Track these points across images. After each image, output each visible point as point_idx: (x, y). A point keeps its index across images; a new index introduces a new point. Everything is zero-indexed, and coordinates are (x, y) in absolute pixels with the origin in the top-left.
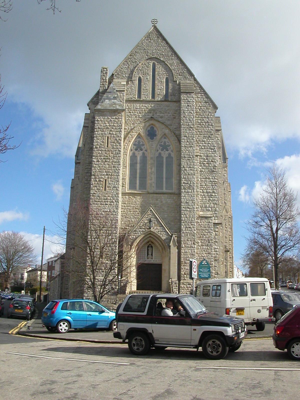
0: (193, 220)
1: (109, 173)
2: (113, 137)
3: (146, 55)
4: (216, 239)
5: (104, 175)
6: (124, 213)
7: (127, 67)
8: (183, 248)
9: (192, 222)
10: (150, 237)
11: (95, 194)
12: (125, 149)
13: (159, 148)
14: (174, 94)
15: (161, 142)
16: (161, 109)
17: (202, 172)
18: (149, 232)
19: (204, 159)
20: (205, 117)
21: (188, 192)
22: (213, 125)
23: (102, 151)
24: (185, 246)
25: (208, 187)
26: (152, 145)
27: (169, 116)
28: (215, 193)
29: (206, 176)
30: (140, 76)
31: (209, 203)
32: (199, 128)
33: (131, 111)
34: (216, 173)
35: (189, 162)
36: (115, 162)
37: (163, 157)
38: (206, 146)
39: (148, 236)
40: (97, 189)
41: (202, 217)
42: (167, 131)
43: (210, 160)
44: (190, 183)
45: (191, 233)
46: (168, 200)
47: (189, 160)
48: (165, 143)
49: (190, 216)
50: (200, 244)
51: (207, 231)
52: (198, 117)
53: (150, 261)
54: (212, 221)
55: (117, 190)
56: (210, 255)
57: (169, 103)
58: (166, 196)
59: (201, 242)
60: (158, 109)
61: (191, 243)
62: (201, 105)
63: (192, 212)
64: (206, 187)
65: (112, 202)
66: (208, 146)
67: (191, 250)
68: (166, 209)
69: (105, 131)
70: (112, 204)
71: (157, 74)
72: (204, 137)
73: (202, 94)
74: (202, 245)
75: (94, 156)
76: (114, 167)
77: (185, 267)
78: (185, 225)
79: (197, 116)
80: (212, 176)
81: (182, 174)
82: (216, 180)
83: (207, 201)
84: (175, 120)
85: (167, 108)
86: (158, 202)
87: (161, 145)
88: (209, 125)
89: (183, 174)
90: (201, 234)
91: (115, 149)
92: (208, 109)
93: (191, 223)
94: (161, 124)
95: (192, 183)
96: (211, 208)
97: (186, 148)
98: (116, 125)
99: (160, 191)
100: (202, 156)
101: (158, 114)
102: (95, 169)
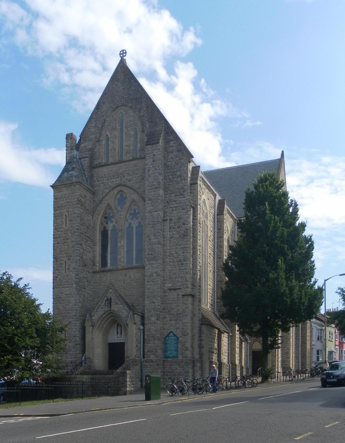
4: (185, 312)
6: (96, 293)
8: (146, 324)
9: (156, 296)
10: (112, 316)
12: (94, 225)
15: (131, 211)
16: (129, 171)
17: (173, 239)
18: (110, 312)
22: (185, 179)
23: (62, 231)
24: (149, 323)
28: (185, 261)
29: (176, 243)
30: (107, 133)
31: (180, 273)
32: (170, 186)
33: (100, 180)
34: (187, 237)
35: (154, 229)
37: (133, 227)
38: (176, 207)
39: (111, 315)
41: (170, 290)
42: (135, 196)
45: (155, 308)
47: (153, 227)
48: (135, 210)
51: (175, 305)
52: (170, 172)
53: (120, 340)
57: (137, 161)
58: (135, 270)
60: (127, 171)
61: (155, 319)
62: (172, 156)
67: (155, 326)
71: (125, 126)
73: (174, 142)
74: (171, 320)
77: (148, 344)
78: (148, 300)
79: (168, 171)
80: (183, 241)
81: (146, 245)
82: (187, 246)
87: (131, 214)
89: (147, 244)
90: (169, 308)
96: (181, 278)
99: (130, 266)
102: (56, 252)
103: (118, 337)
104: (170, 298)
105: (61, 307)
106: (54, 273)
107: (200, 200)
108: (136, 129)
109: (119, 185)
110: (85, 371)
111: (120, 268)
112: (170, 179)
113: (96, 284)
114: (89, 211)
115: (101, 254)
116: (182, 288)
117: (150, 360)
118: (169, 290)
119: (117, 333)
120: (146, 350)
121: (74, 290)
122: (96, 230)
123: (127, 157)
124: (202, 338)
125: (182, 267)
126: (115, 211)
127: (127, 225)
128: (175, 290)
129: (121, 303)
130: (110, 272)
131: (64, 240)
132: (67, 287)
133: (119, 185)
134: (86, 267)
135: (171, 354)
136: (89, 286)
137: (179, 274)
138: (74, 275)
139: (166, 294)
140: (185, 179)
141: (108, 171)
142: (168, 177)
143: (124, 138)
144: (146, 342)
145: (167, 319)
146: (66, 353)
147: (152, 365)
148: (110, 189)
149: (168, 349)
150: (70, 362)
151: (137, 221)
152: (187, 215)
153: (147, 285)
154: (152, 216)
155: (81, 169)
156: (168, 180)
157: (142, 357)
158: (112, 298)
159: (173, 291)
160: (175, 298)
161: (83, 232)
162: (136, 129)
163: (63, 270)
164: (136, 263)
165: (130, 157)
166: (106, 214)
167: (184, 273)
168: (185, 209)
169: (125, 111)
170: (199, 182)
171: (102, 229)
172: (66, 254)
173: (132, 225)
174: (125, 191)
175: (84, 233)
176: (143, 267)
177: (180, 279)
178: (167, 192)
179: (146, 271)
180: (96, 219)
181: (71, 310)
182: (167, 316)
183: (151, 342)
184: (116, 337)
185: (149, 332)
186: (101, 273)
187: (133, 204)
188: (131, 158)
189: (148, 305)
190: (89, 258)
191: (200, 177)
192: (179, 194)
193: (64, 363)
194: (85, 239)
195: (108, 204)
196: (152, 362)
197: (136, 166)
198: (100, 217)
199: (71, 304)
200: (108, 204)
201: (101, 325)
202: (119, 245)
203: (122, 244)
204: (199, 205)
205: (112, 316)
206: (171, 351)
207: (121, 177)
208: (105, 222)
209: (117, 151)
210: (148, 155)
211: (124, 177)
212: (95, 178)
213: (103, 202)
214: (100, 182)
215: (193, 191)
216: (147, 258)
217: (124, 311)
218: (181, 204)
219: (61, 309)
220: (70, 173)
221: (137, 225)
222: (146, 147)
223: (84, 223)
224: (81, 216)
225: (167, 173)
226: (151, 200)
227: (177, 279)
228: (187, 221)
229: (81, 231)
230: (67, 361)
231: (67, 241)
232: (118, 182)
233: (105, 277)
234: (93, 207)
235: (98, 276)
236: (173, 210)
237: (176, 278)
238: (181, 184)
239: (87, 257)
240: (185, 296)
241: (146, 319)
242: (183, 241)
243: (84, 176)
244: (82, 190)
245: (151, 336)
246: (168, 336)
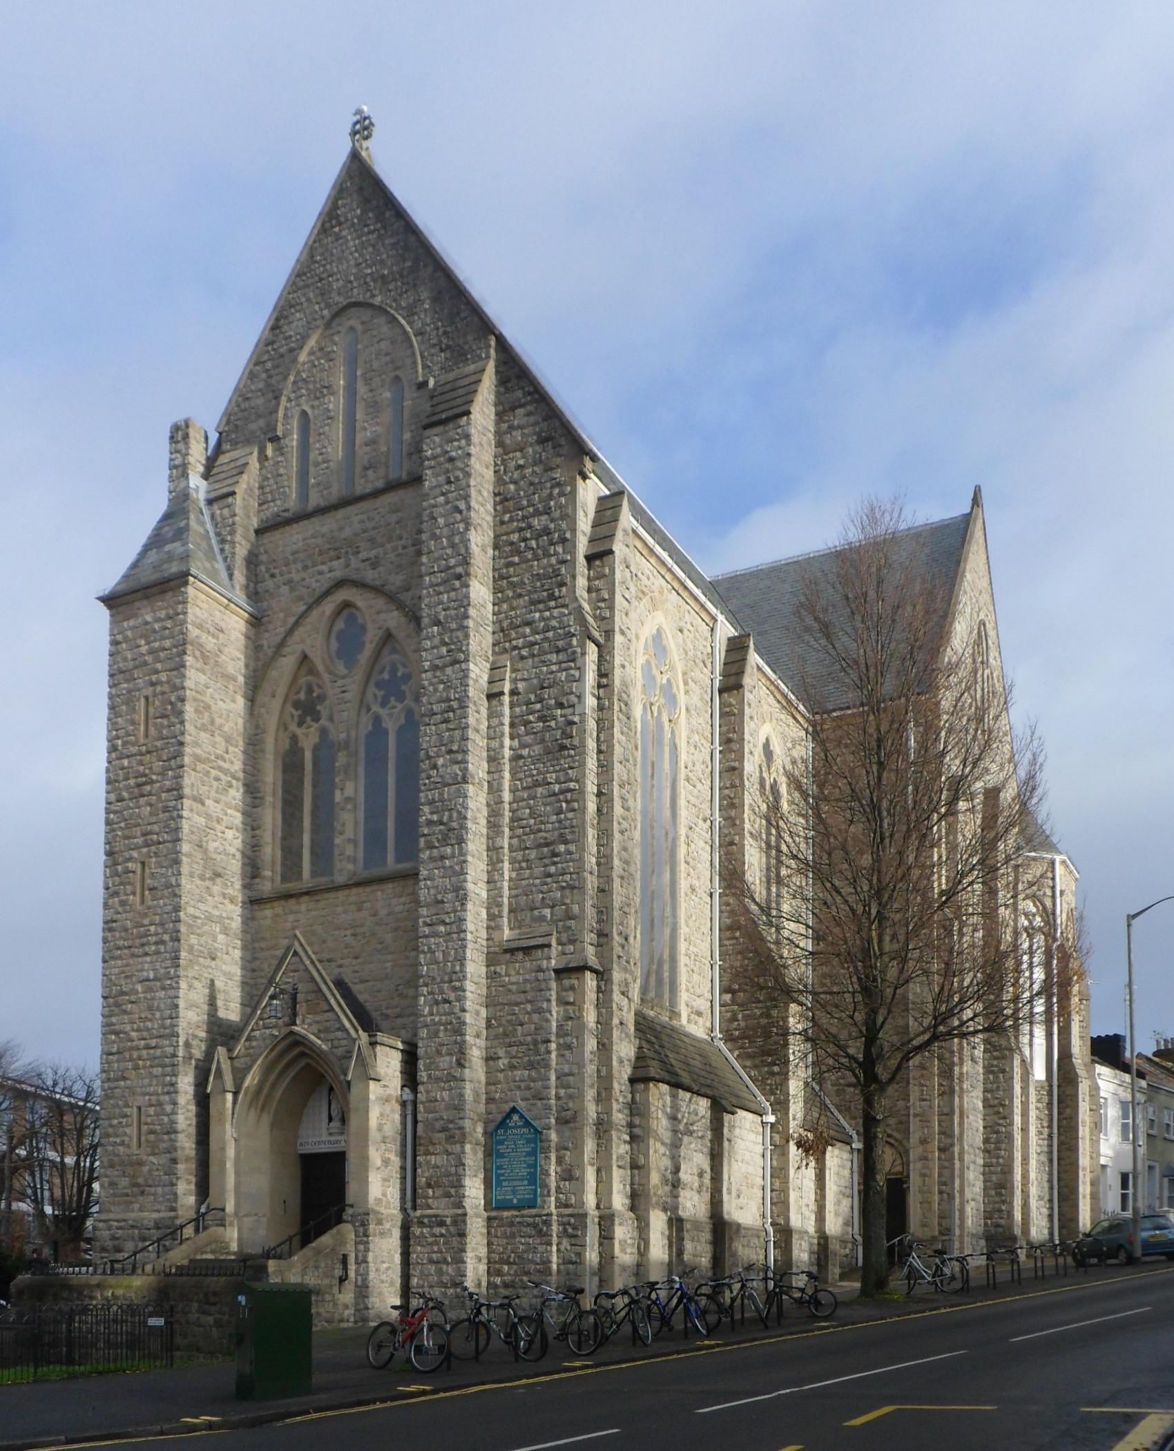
0: (458, 968)
3: (322, 305)
4: (567, 1035)
5: (137, 848)
10: (303, 1054)
11: (115, 921)
13: (375, 696)
15: (382, 672)
16: (374, 528)
17: (521, 763)
18: (291, 1039)
19: (528, 703)
20: (537, 513)
21: (443, 858)
24: (429, 1076)
25: (542, 822)
26: (344, 692)
27: (400, 551)
28: (566, 842)
34: (572, 752)
35: (449, 730)
37: (386, 732)
38: (535, 644)
41: (512, 951)
42: (393, 619)
43: (553, 702)
44: (451, 817)
45: (451, 1023)
46: (395, 901)
47: (446, 721)
49: (449, 954)
50: (502, 1063)
51: (529, 1007)
52: (511, 520)
54: (549, 962)
55: (175, 895)
56: (539, 1103)
57: (401, 493)
58: (390, 885)
59: (507, 1052)
60: (364, 532)
63: (455, 936)
64: (532, 821)
65: (163, 942)
66: (546, 639)
67: (450, 1089)
68: (388, 937)
70: (162, 948)
72: (533, 602)
74: (512, 1067)
78: (429, 993)
79: (507, 517)
80: (557, 768)
82: (572, 785)
83: (538, 881)
86: (365, 913)
87: (379, 685)
88: (552, 544)
93: (451, 981)
94: (371, 595)
95: (455, 815)
96: (552, 907)
97: (438, 673)
99: (376, 872)
100: (519, 694)
101: (363, 555)
103: (330, 1134)
104: (512, 984)
106: (106, 906)
107: (627, 614)
108: (397, 379)
109: (340, 584)
110: (199, 1257)
111: (340, 879)
112: (512, 543)
113: (263, 945)
114: (235, 680)
115: (280, 834)
116: (554, 943)
117: (436, 1216)
118: (506, 951)
119: (330, 1119)
120: (422, 1181)
122: (263, 751)
123: (367, 482)
124: (637, 1131)
125: (554, 863)
126: (326, 677)
127: (366, 726)
128: (527, 950)
129: (330, 1004)
130: (306, 898)
131: (139, 785)
132: (146, 954)
133: (340, 584)
134: (218, 880)
135: (514, 1192)
136: (230, 949)
137: (542, 892)
139: (498, 969)
140: (567, 542)
141: (304, 539)
142: (505, 538)
143: (358, 416)
144: (421, 1150)
145: (500, 1062)
146: (143, 1193)
147: (442, 1235)
148: (311, 600)
149: (503, 1175)
150: (152, 1224)
151: (400, 706)
152: (572, 672)
153: (426, 937)
154: (442, 682)
155: (212, 534)
156: (507, 549)
157: (409, 1205)
158: (300, 986)
159: (520, 955)
160: (526, 981)
161: (209, 753)
162: (397, 378)
163: (134, 893)
164: (398, 860)
165: (375, 480)
166: (298, 693)
167: (563, 888)
168: (566, 650)
169: (363, 323)
170: (618, 547)
171: (286, 744)
172: (144, 835)
173: (384, 725)
174: (359, 604)
175: (213, 757)
176: (414, 875)
177: (547, 912)
178: (501, 592)
179: (422, 884)
180: (263, 710)
182: (501, 1053)
183: (439, 1148)
184: (324, 1132)
185: (431, 1112)
186: (275, 904)
187: (386, 650)
188: (380, 484)
189: (427, 1010)
190: (232, 850)
191: (625, 530)
192: (545, 594)
193: (132, 1227)
194: (217, 779)
195: (305, 658)
196: (442, 1224)
197: (398, 511)
198: (276, 704)
199: (158, 1015)
200: (305, 658)
201: (265, 1091)
202: (338, 796)
203: (349, 790)
204: (622, 633)
205: (303, 1054)
206: (515, 1183)
207: (347, 553)
208: (296, 719)
210: (433, 463)
211: (358, 553)
212: (263, 568)
213: (286, 650)
214: (279, 577)
215: (597, 582)
216: (425, 835)
217: (339, 1034)
218: (550, 634)
220: (167, 548)
221: (402, 721)
222: (428, 432)
223: (212, 722)
224: (199, 696)
225: (502, 523)
227: (536, 912)
229: (199, 751)
230: (145, 1222)
231: (148, 788)
232: (338, 574)
233: (291, 918)
234: (255, 671)
235: (268, 913)
236: (522, 658)
237: (532, 909)
238: (553, 560)
239: (228, 847)
240: (564, 975)
241: (421, 1064)
242: (557, 768)
243: (219, 558)
244: (205, 606)
245: (438, 1125)
246: (502, 1124)
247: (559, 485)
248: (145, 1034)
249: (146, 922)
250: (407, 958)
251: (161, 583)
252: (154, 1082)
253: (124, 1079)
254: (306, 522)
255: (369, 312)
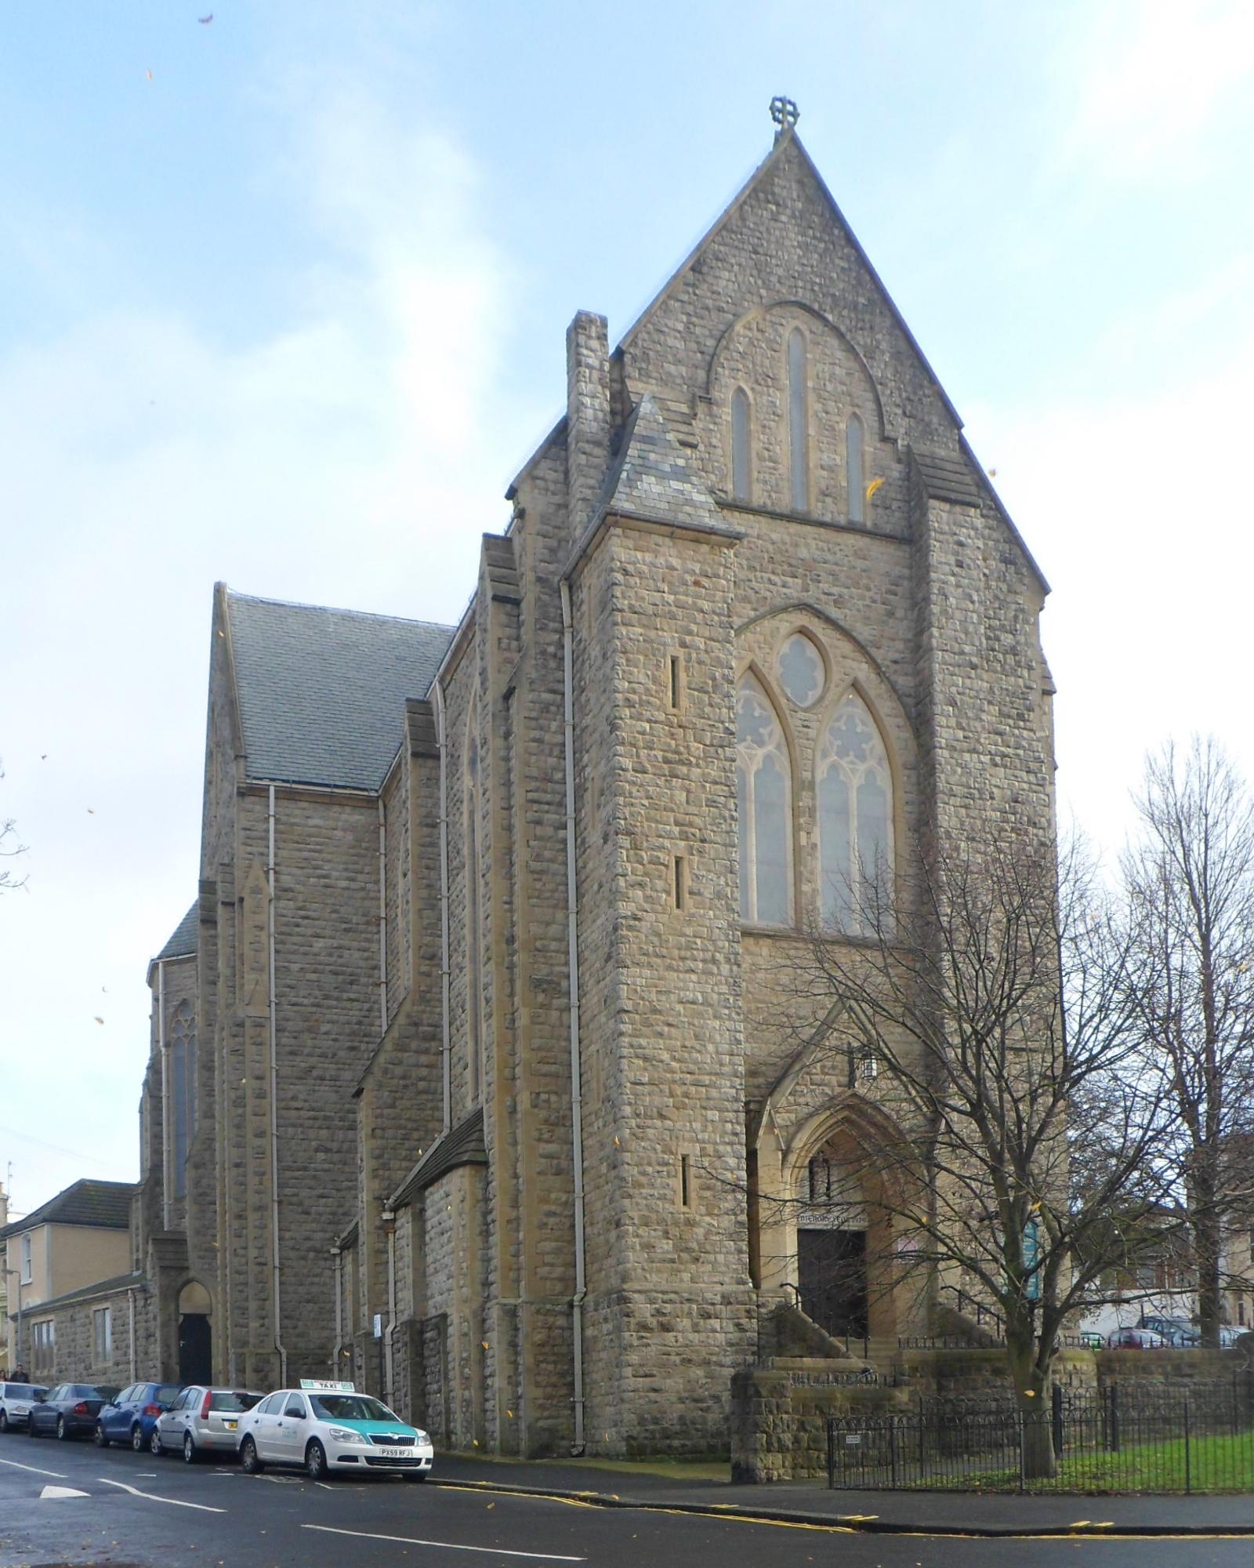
1: (693, 830)
2: (700, 662)
7: (680, 327)
14: (888, 502)
20: (1002, 628)
23: (656, 722)
36: (716, 783)
40: (647, 898)
65: (714, 961)
69: (663, 630)
71: (814, 388)
75: (623, 744)
76: (711, 803)
84: (891, 621)
85: (860, 564)
91: (709, 719)
92: (1016, 593)
98: (706, 605)
105: (666, 1056)
121: (724, 989)
138: (723, 923)
143: (812, 431)
172: (677, 823)
181: (716, 1074)
188: (842, 520)
192: (1015, 711)
199: (711, 1048)
209: (783, 469)
218: (1021, 752)
219: (662, 1061)
226: (953, 704)
228: (1043, 816)
247: (1023, 611)
248: (692, 1067)
249: (689, 931)
250: (892, 1033)
251: (699, 531)
252: (710, 1128)
253: (662, 1117)
254: (751, 517)
255: (817, 326)
